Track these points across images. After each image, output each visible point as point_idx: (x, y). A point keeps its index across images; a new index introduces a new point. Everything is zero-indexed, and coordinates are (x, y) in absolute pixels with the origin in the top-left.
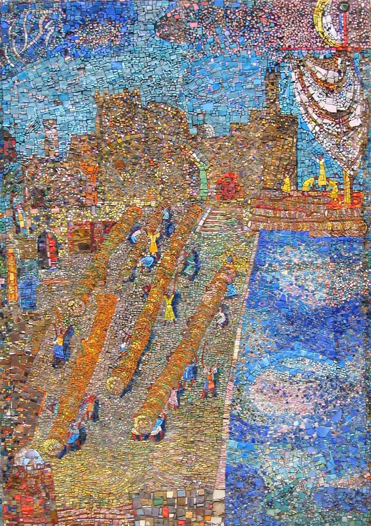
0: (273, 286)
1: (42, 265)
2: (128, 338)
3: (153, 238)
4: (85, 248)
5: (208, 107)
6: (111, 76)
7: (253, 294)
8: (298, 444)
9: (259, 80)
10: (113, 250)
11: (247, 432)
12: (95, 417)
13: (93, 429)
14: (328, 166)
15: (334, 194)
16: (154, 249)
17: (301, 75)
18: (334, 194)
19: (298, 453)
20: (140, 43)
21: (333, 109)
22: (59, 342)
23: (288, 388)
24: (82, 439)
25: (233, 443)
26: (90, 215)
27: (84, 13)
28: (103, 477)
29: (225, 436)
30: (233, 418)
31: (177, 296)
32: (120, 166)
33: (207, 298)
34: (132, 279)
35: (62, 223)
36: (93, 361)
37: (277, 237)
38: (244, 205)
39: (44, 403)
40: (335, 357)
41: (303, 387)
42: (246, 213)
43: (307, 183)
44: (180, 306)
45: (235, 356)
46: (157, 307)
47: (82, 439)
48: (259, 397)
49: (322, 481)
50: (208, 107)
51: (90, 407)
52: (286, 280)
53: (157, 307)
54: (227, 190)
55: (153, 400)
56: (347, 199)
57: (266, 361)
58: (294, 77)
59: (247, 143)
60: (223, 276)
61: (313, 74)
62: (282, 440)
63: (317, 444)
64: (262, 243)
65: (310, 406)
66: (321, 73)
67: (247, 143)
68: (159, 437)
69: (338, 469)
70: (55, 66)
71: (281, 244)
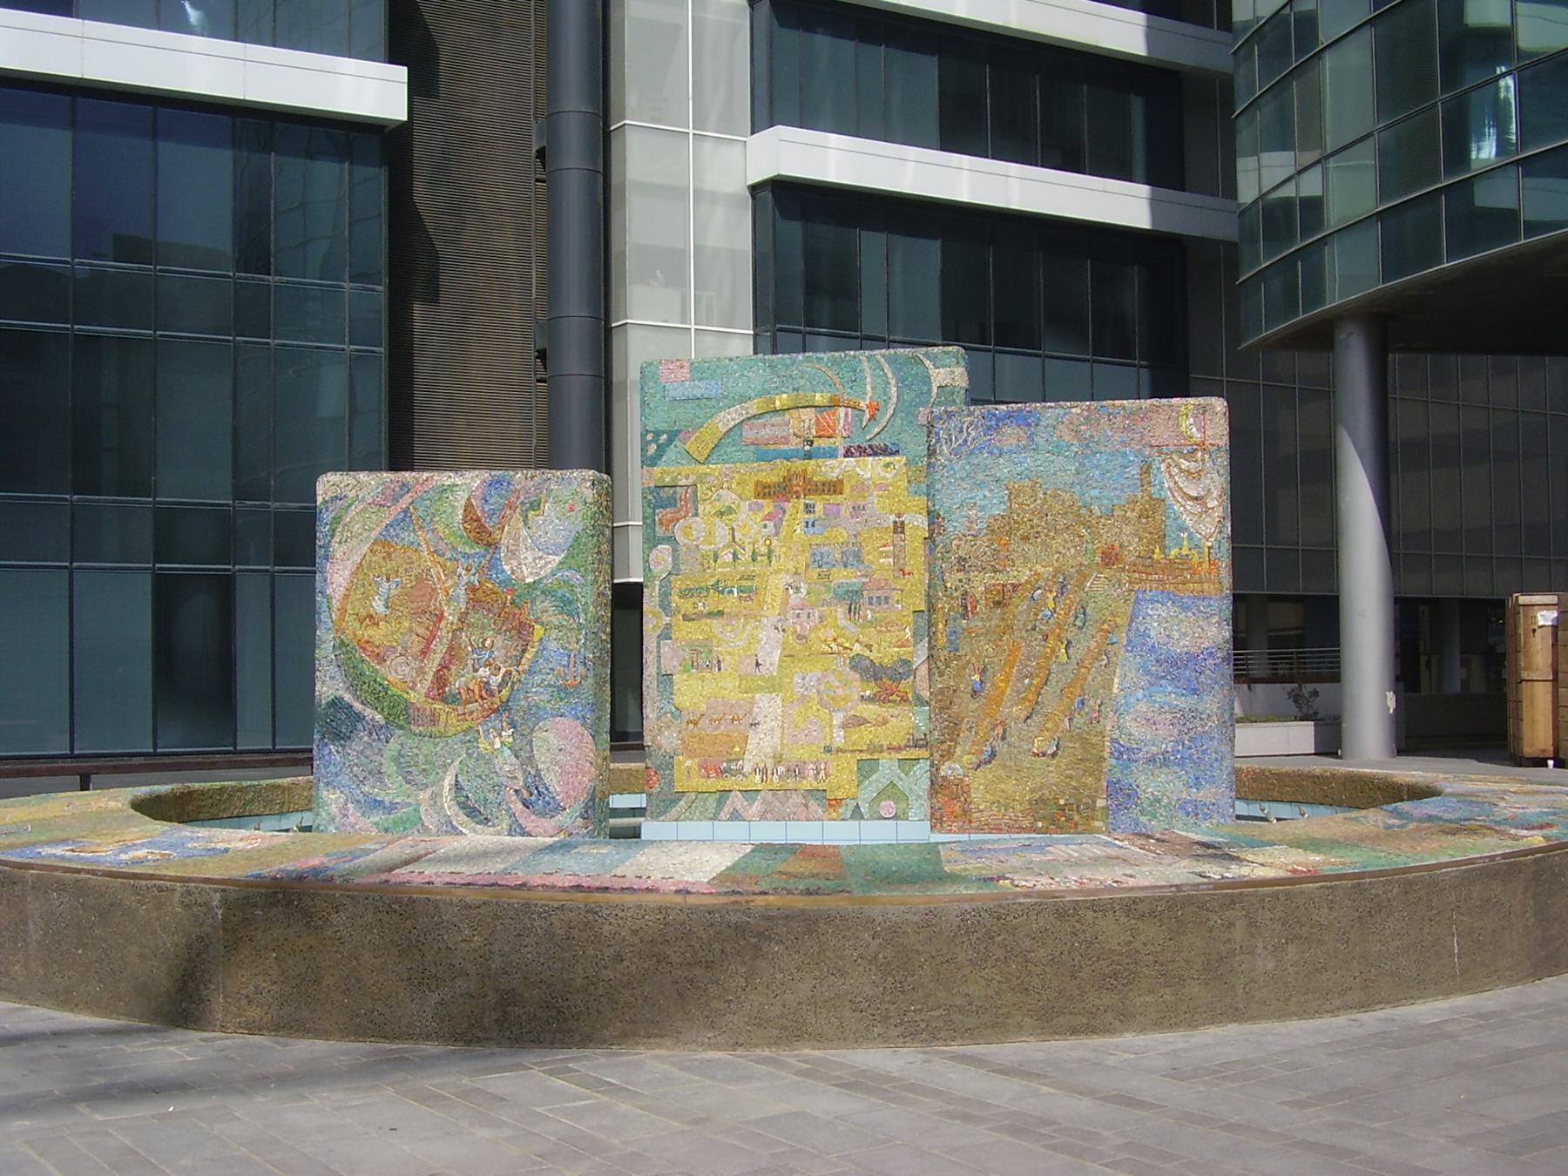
0: (1145, 635)
1: (964, 616)
2: (1030, 676)
3: (1051, 596)
4: (997, 604)
5: (1095, 492)
6: (1019, 469)
7: (1129, 641)
8: (1165, 763)
9: (1134, 470)
10: (1020, 606)
11: (1125, 753)
12: (1003, 738)
13: (1001, 748)
14: (1190, 538)
15: (1195, 560)
16: (1051, 605)
17: (1169, 466)
18: (1195, 560)
19: (1165, 770)
20: (1042, 442)
21: (1194, 494)
22: (976, 677)
23: (1157, 718)
24: (993, 755)
25: (1114, 761)
26: (1002, 578)
27: (998, 420)
28: (1009, 786)
29: (1106, 755)
30: (1113, 741)
31: (1069, 643)
32: (1025, 538)
33: (1093, 645)
34: (1034, 629)
35: (980, 584)
36: (1003, 693)
37: (1149, 595)
38: (1123, 569)
39: (964, 727)
40: (1195, 692)
41: (1169, 717)
42: (1125, 577)
43: (1174, 552)
44: (1071, 651)
45: (1115, 691)
46: (1053, 651)
47: (993, 755)
48: (1134, 724)
49: (1184, 795)
50: (1095, 492)
51: (1000, 730)
52: (1155, 631)
53: (1053, 651)
54: (1110, 558)
55: (1049, 725)
56: (1206, 565)
57: (1140, 694)
58: (1163, 467)
59: (1126, 521)
60: (1105, 626)
61: (1178, 465)
62: (1152, 760)
63: (1181, 764)
64: (1137, 601)
65: (1176, 732)
66: (1185, 464)
67: (1126, 521)
68: (1054, 755)
69: (1197, 784)
70: (976, 461)
71: (1152, 601)
